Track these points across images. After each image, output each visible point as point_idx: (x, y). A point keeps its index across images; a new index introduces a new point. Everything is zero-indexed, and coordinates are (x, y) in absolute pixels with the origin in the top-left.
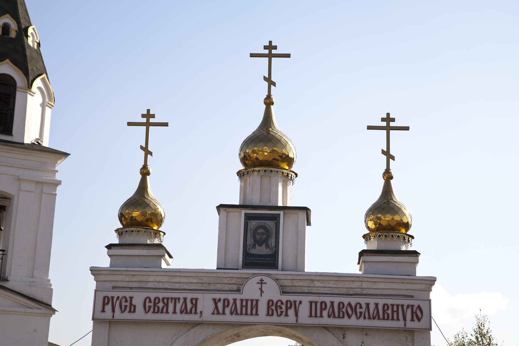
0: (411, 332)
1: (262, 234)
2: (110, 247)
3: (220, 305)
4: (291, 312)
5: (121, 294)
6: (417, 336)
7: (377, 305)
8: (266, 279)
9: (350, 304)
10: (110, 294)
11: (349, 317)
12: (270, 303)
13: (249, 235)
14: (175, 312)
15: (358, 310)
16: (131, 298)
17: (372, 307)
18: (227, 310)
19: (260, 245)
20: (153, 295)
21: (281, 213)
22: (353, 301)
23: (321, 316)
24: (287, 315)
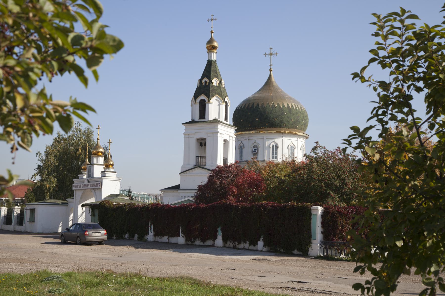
2: (102, 172)
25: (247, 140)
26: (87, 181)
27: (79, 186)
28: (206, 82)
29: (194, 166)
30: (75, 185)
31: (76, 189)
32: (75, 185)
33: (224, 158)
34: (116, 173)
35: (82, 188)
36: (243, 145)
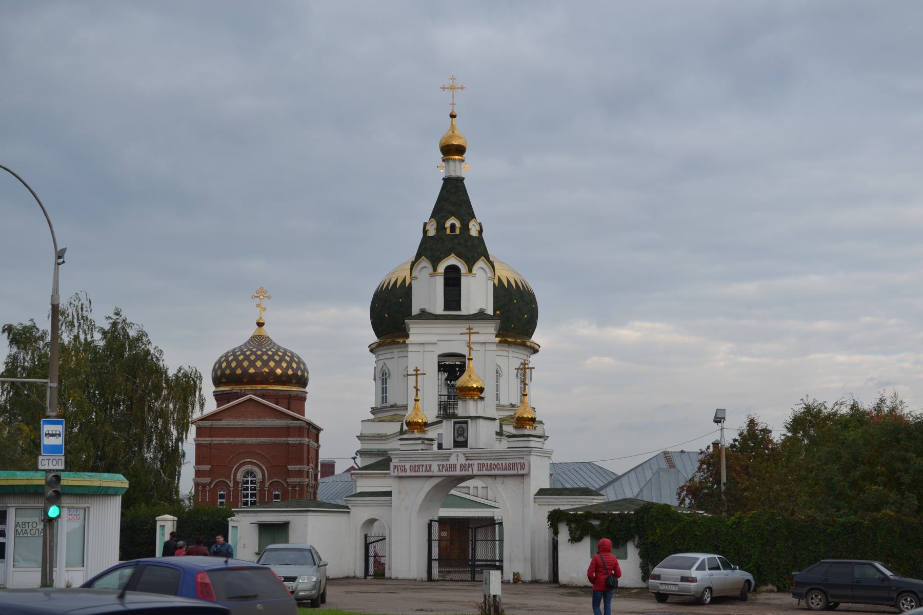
0: (523, 475)
1: (461, 431)
3: (441, 467)
4: (470, 469)
5: (400, 464)
6: (525, 477)
7: (506, 463)
8: (459, 454)
9: (494, 464)
10: (396, 464)
11: (494, 470)
12: (461, 465)
13: (455, 432)
14: (422, 471)
15: (498, 466)
16: (405, 465)
17: (504, 465)
18: (444, 470)
19: (460, 436)
20: (413, 464)
21: (469, 420)
22: (496, 462)
23: (483, 470)
24: (468, 470)
28: (453, 227)
29: (437, 417)
35: (436, 473)
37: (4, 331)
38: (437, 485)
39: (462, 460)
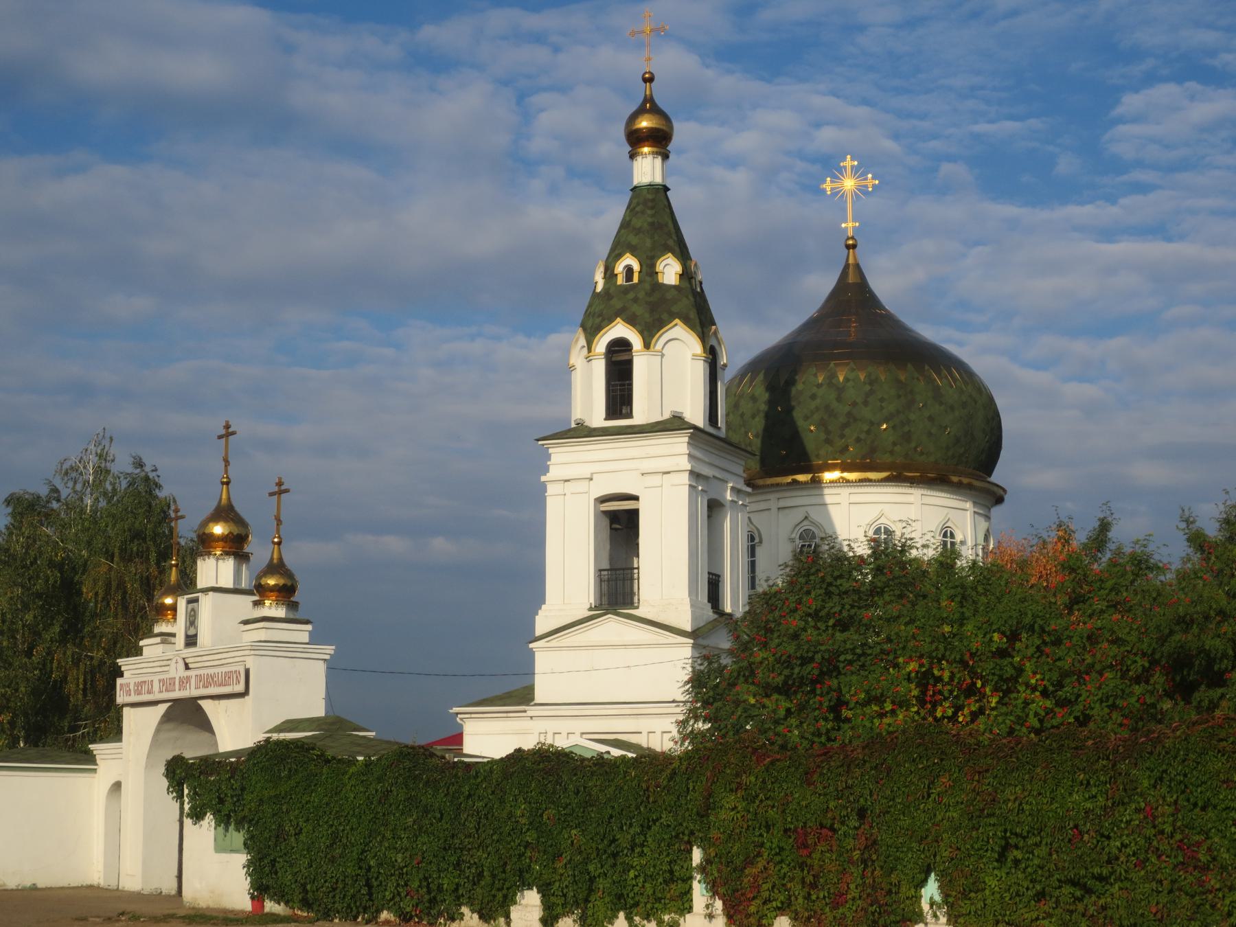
15: (215, 679)
20: (137, 680)
21: (199, 594)
22: (211, 671)
25: (774, 510)
26: (181, 665)
27: (145, 688)
28: (629, 270)
29: (590, 609)
30: (128, 685)
31: (134, 698)
32: (128, 685)
33: (709, 573)
34: (309, 627)
36: (758, 530)
37: (8, 502)
38: (167, 718)
39: (182, 672)
